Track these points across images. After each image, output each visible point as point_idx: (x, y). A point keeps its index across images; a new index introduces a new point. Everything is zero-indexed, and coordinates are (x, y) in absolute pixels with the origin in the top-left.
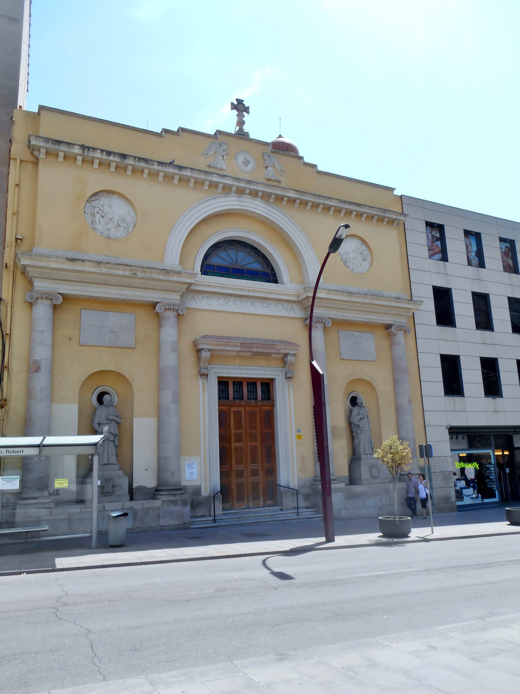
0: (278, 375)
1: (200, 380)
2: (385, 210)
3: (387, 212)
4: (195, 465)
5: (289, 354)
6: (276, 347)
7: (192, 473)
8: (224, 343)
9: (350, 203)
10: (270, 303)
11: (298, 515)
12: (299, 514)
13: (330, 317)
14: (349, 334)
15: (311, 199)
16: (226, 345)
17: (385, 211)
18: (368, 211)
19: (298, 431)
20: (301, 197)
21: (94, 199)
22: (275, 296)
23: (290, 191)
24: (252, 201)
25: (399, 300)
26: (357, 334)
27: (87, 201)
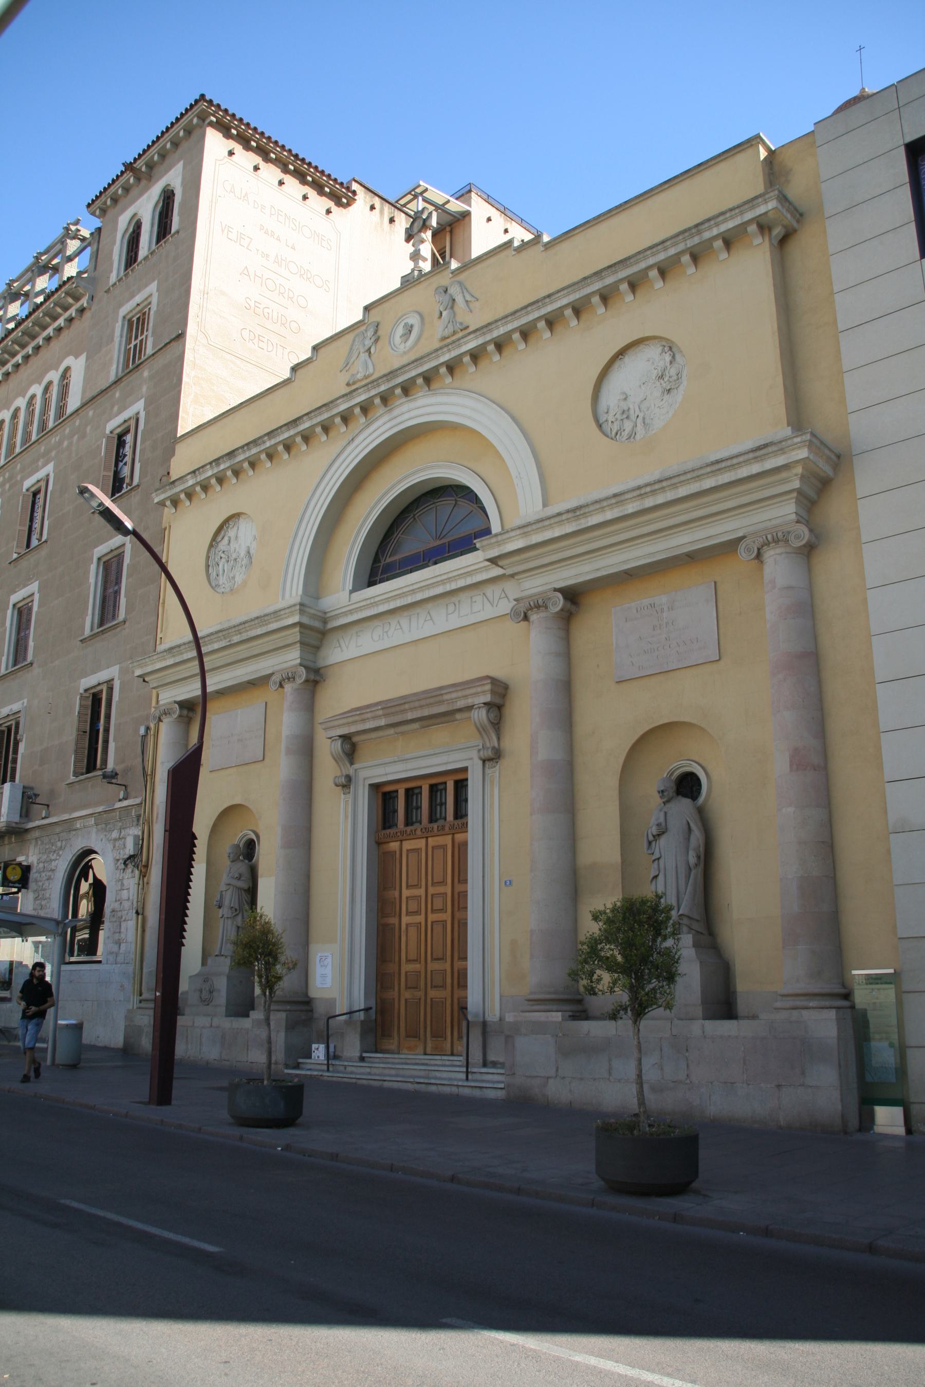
0: (471, 759)
1: (343, 796)
2: (697, 226)
3: (707, 225)
4: (329, 960)
5: (474, 706)
6: (446, 697)
7: (324, 976)
8: (357, 718)
9: (598, 274)
10: (459, 601)
11: (467, 1079)
12: (470, 1077)
13: (558, 586)
14: (639, 609)
15: (510, 327)
16: (363, 720)
17: (698, 231)
18: (651, 261)
19: (506, 882)
20: (488, 337)
21: (219, 539)
22: (461, 583)
23: (465, 340)
24: (412, 405)
25: (723, 465)
26: (662, 600)
27: (211, 546)
